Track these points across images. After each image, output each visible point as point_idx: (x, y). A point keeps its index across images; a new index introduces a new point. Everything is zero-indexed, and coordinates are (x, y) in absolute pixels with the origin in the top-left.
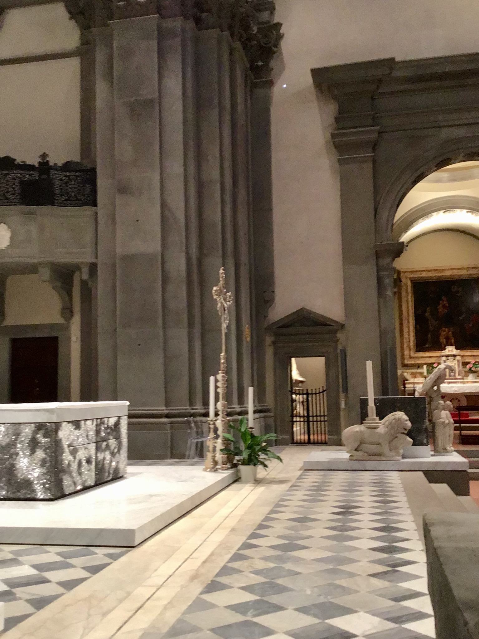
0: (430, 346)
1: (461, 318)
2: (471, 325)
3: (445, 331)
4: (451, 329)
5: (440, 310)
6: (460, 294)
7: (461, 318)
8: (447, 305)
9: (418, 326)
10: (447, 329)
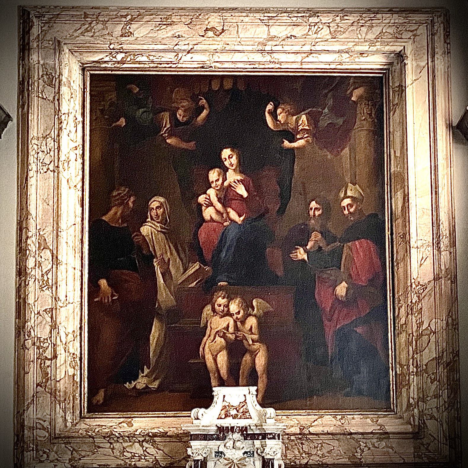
0: (155, 385)
1: (301, 254)
2: (341, 289)
3: (229, 314)
4: (254, 303)
5: (208, 213)
6: (301, 143)
7: (301, 254)
8: (242, 190)
9: (103, 283)
10: (234, 307)
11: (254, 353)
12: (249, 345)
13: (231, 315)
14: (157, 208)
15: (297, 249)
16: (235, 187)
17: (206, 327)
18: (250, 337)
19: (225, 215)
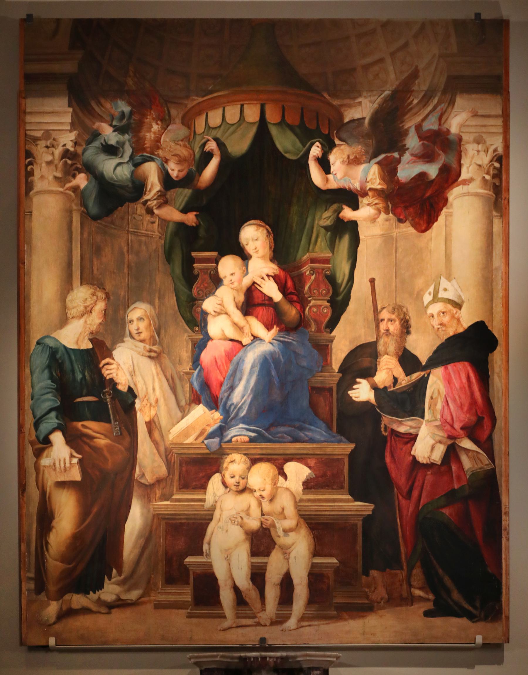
11: (286, 551)
12: (279, 536)
13: (252, 491)
14: (140, 319)
15: (359, 383)
16: (261, 285)
17: (213, 509)
18: (281, 525)
19: (246, 330)
